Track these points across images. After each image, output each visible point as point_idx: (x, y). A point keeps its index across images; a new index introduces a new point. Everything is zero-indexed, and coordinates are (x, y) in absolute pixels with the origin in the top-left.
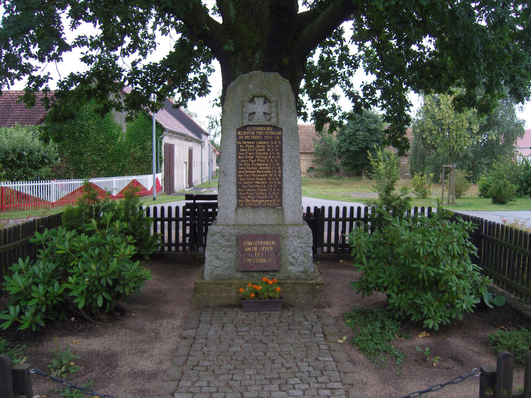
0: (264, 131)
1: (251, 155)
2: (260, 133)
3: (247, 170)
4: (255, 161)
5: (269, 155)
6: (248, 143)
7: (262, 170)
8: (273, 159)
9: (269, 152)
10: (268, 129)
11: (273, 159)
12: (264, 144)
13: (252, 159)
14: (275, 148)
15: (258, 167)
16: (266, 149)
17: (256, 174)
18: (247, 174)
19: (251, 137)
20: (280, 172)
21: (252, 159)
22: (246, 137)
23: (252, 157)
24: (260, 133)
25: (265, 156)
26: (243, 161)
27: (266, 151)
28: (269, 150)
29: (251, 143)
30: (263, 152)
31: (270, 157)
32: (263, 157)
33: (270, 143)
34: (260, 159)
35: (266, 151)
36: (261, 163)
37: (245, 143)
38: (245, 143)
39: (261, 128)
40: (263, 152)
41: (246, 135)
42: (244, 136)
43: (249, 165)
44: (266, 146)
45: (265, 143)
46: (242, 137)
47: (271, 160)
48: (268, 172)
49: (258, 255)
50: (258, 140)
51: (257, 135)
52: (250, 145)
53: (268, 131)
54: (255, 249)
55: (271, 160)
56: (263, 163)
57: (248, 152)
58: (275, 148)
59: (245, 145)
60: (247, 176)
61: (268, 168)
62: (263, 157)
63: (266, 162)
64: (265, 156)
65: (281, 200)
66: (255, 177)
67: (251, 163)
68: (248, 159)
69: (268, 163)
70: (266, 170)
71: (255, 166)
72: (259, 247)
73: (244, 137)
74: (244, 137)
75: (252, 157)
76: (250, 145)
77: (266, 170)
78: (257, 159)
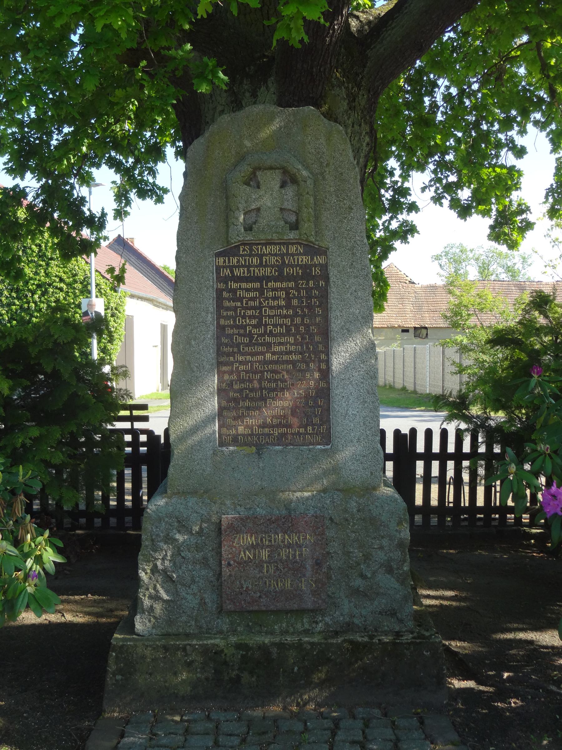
0: (282, 256)
1: (250, 317)
2: (273, 260)
3: (243, 354)
4: (262, 330)
5: (296, 315)
6: (244, 285)
7: (281, 353)
8: (307, 326)
9: (294, 308)
10: (293, 249)
11: (307, 326)
12: (282, 289)
13: (254, 326)
14: (309, 297)
15: (269, 345)
16: (288, 299)
17: (265, 362)
18: (241, 363)
19: (249, 271)
20: (323, 356)
21: (254, 326)
22: (236, 272)
23: (254, 322)
24: (273, 260)
25: (286, 317)
26: (231, 332)
27: (288, 306)
28: (295, 302)
29: (250, 285)
30: (279, 307)
31: (298, 320)
32: (281, 321)
33: (297, 285)
34: (275, 326)
35: (288, 306)
36: (275, 335)
37: (234, 285)
38: (234, 285)
39: (275, 249)
40: (279, 307)
41: (239, 267)
42: (231, 268)
43: (246, 340)
44: (288, 294)
45: (284, 285)
46: (228, 272)
47: (302, 329)
48: (294, 357)
49: (272, 571)
50: (268, 279)
51: (266, 266)
52: (248, 290)
53: (293, 255)
54: (264, 554)
55: (302, 329)
56: (281, 335)
57: (243, 308)
58: (309, 297)
59: (234, 291)
60: (242, 367)
61: (293, 348)
62: (281, 321)
63: (288, 333)
64: (286, 317)
65: (329, 429)
66: (262, 372)
67: (251, 335)
68: (244, 327)
69: (294, 335)
70: (290, 353)
71: (262, 345)
72: (274, 549)
73: (232, 272)
74: (232, 272)
75: (254, 322)
76: (248, 290)
77: (290, 353)
78: (266, 325)
